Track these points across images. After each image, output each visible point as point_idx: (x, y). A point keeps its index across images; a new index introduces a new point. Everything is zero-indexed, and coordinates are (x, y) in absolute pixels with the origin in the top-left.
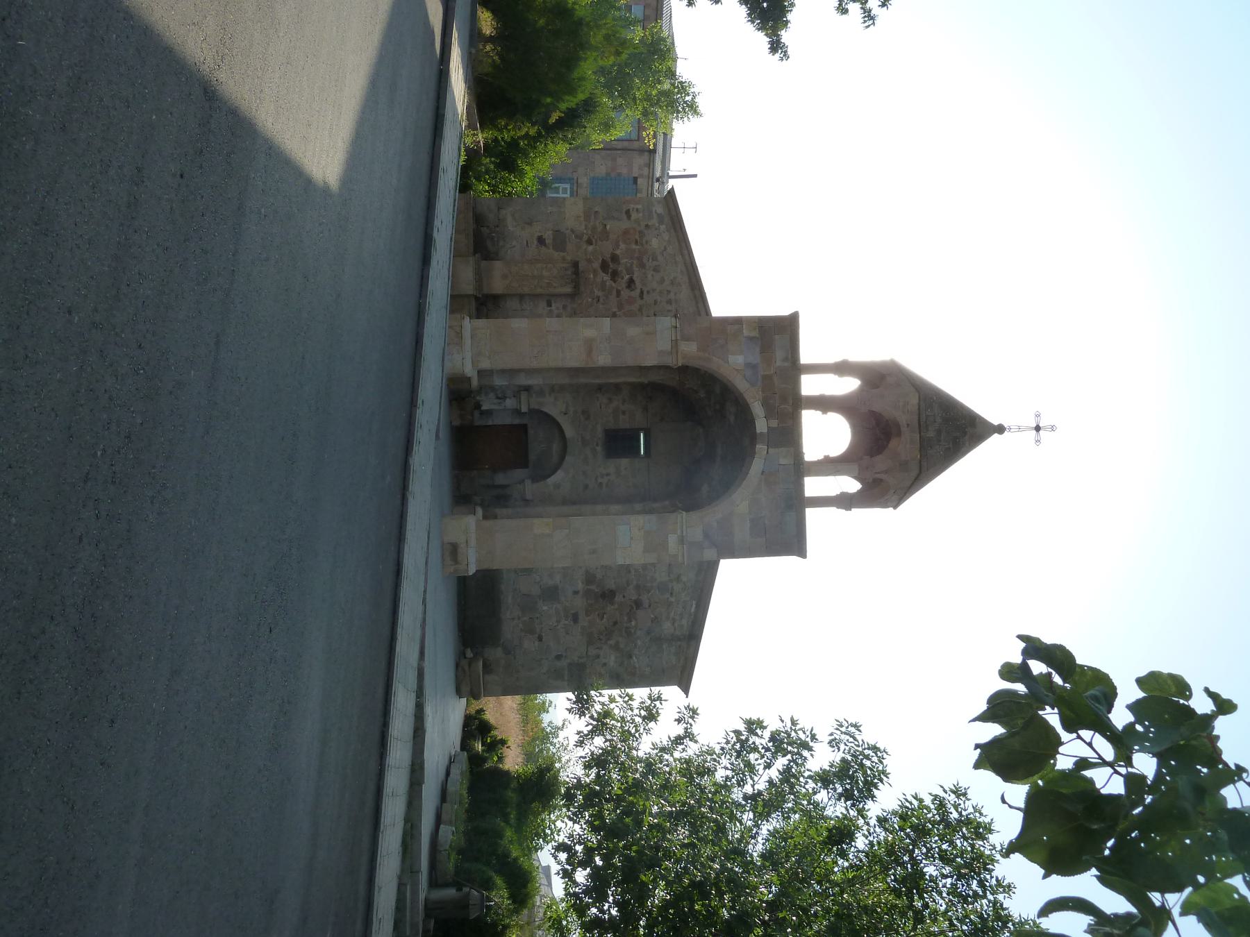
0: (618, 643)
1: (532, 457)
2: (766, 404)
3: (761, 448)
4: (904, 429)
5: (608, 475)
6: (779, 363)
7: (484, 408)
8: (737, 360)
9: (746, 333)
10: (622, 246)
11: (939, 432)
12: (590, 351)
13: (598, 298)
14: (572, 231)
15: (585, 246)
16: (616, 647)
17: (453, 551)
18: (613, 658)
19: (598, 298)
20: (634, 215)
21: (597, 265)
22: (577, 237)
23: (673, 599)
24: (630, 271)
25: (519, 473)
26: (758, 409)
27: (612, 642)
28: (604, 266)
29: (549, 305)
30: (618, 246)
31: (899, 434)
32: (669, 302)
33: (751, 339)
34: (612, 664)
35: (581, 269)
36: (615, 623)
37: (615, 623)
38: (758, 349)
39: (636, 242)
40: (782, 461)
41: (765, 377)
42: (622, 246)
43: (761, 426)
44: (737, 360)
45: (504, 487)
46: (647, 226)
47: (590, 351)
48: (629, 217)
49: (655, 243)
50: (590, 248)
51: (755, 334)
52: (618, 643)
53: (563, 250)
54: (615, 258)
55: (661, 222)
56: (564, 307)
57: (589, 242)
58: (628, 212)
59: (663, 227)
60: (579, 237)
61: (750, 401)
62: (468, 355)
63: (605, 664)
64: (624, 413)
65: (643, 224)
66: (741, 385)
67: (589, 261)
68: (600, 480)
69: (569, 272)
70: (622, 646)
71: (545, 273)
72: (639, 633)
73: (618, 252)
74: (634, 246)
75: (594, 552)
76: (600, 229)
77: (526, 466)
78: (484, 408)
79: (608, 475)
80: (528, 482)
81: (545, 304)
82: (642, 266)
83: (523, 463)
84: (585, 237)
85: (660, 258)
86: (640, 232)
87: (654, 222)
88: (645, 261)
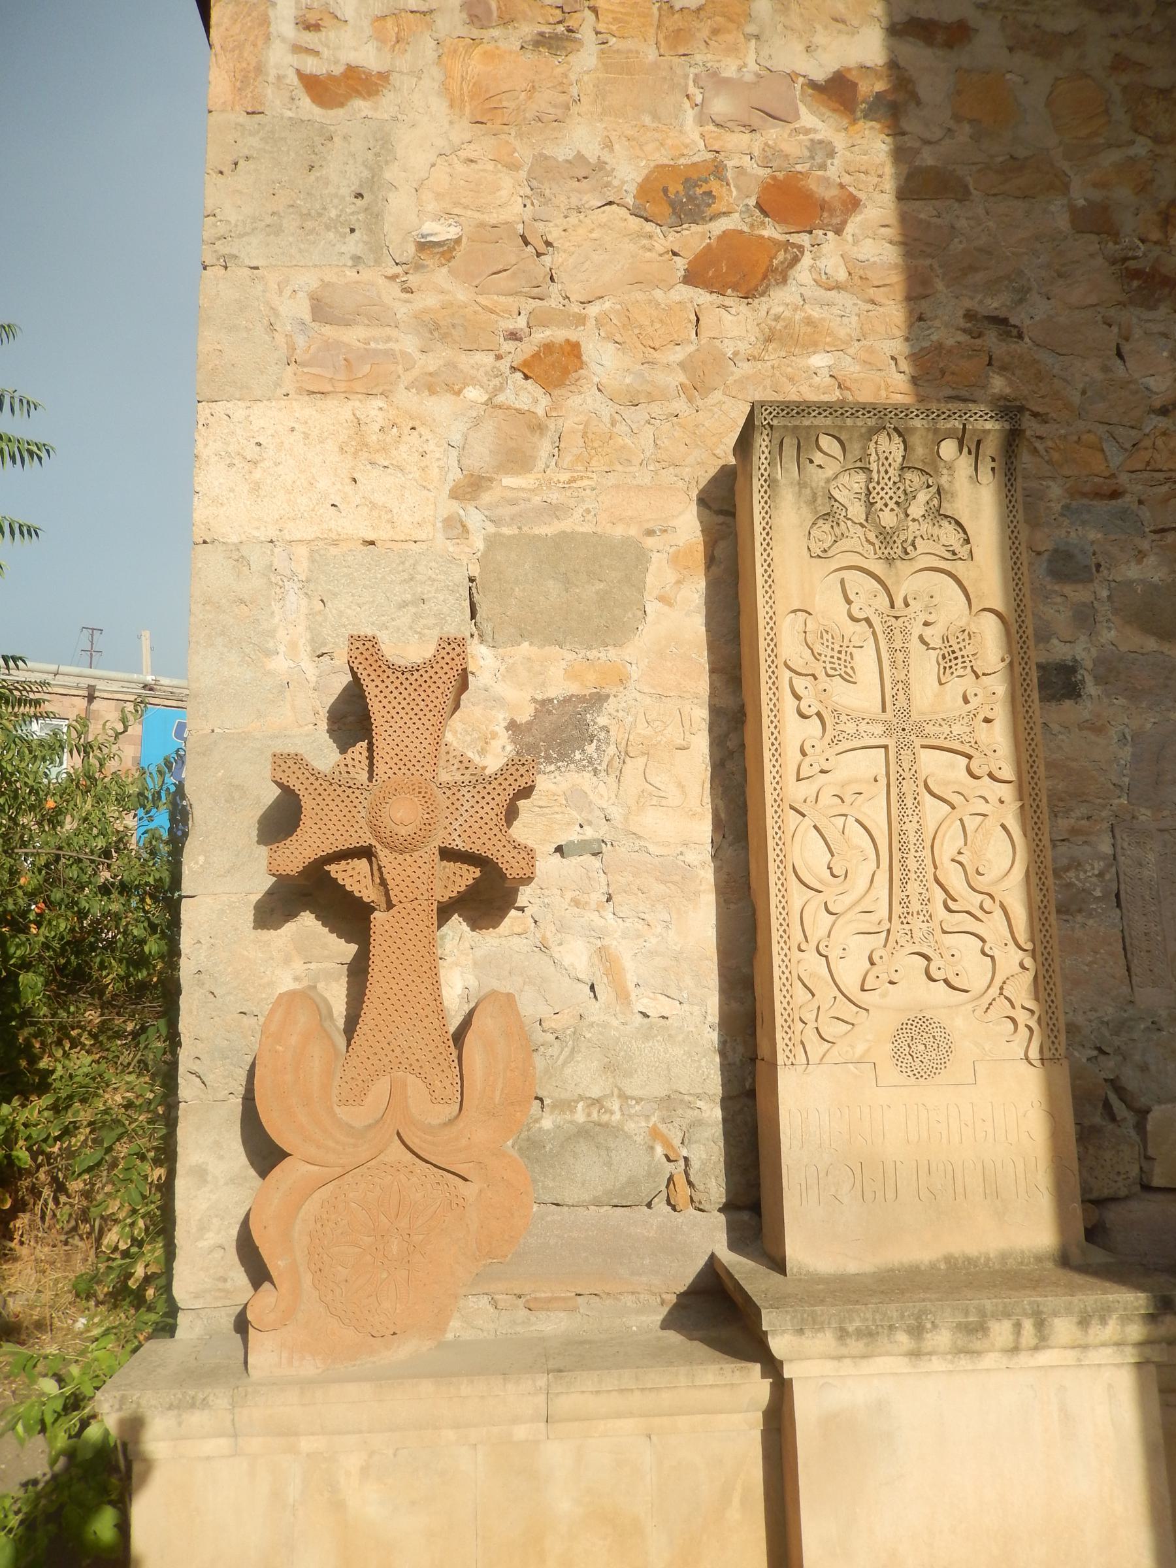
10: (582, 138)
14: (471, 487)
15: (582, 404)
19: (977, 323)
21: (734, 323)
22: (516, 459)
28: (738, 272)
30: (588, 172)
42: (582, 138)
48: (357, 83)
50: (603, 359)
53: (632, 559)
54: (678, 197)
57: (556, 366)
58: (320, 89)
71: (861, 695)
73: (628, 174)
76: (442, 287)
84: (526, 396)
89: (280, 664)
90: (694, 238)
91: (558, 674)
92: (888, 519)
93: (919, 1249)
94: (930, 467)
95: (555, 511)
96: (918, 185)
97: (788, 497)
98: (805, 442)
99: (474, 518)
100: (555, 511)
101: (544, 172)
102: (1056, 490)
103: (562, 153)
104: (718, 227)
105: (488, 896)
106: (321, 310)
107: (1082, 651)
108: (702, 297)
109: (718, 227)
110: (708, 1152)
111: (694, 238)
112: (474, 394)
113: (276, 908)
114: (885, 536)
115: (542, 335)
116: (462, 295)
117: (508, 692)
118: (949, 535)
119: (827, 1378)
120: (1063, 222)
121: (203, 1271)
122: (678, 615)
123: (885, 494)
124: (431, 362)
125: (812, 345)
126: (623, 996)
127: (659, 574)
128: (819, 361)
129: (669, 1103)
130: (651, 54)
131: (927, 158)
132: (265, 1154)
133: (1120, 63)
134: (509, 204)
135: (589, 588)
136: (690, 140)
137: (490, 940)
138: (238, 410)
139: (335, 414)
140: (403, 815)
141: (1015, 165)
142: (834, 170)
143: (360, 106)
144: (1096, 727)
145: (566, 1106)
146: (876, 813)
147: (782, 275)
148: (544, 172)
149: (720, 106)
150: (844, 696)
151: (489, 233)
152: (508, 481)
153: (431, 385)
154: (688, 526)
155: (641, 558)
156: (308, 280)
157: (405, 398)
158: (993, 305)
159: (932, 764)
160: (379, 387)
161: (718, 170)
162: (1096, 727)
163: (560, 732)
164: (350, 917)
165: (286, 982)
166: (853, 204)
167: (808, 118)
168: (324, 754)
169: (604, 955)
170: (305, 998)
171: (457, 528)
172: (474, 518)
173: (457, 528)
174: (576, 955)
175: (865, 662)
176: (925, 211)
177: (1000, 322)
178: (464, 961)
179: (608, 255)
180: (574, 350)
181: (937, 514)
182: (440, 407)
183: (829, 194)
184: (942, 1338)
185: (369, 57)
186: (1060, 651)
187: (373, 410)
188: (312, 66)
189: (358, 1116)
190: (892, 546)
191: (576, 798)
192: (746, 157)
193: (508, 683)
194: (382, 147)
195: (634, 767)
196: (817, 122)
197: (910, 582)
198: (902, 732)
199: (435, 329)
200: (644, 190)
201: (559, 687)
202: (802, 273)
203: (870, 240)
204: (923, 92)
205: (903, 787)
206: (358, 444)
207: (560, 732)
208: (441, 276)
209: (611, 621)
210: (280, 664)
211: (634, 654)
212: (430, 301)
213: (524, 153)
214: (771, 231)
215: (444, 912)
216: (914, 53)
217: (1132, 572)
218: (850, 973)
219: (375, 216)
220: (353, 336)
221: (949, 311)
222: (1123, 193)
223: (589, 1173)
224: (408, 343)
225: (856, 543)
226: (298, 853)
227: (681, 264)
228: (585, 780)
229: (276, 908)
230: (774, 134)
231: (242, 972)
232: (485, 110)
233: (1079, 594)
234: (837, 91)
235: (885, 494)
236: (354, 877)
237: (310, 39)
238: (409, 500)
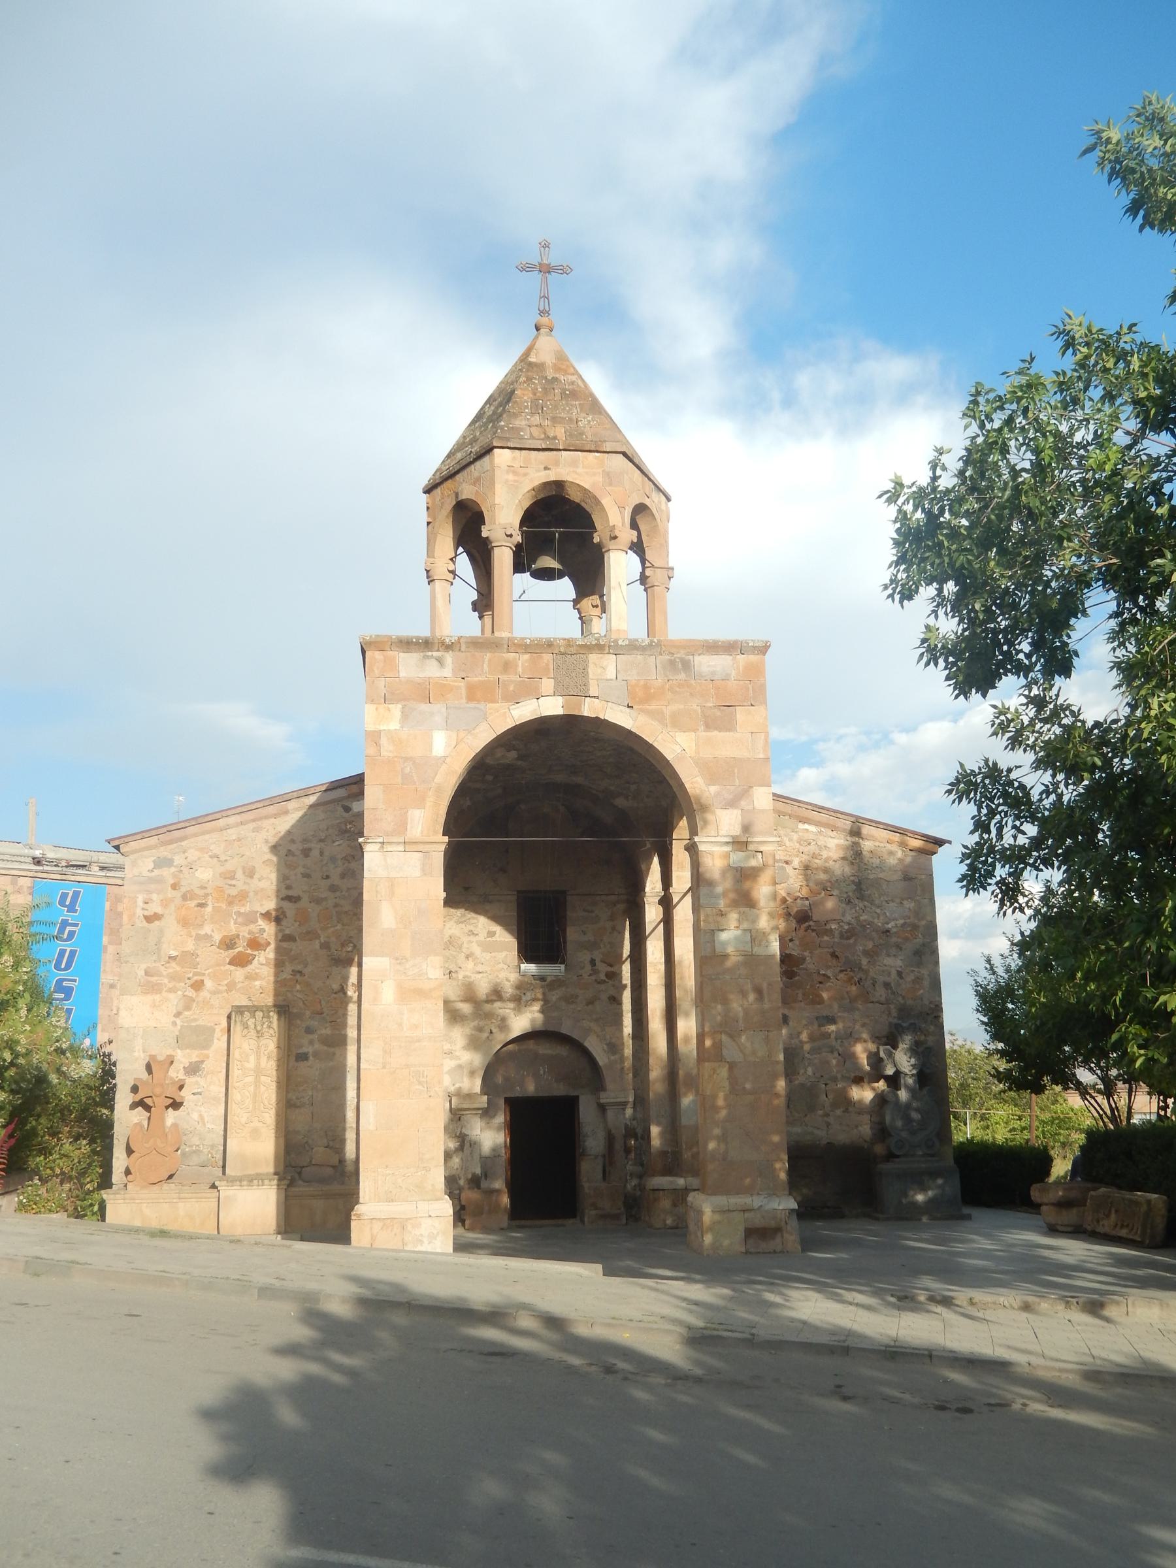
0: (866, 953)
1: (560, 1090)
2: (515, 698)
3: (588, 709)
4: (552, 476)
5: (593, 962)
6: (447, 672)
7: (478, 1171)
8: (440, 743)
9: (394, 725)
10: (207, 929)
11: (555, 420)
12: (421, 993)
13: (295, 972)
14: (178, 1015)
15: (204, 994)
16: (871, 954)
17: (760, 1234)
18: (889, 961)
19: (295, 972)
20: (155, 908)
21: (239, 973)
22: (188, 1008)
23: (796, 862)
24: (250, 919)
25: (587, 1112)
26: (525, 712)
27: (864, 961)
28: (240, 961)
29: (302, 1057)
30: (207, 937)
31: (559, 485)
32: (306, 853)
33: (405, 716)
34: (899, 963)
35: (243, 1001)
36: (834, 955)
37: (834, 955)
38: (424, 707)
39: (201, 905)
40: (611, 673)
41: (471, 697)
43: (552, 706)
44: (440, 743)
45: (610, 1139)
46: (174, 887)
47: (421, 993)
49: (205, 874)
50: (209, 984)
51: (396, 709)
52: (866, 953)
53: (212, 1030)
54: (228, 943)
55: (168, 862)
56: (309, 1031)
57: (198, 986)
58: (149, 919)
59: (178, 860)
60: (188, 1004)
61: (510, 724)
62: (424, 1207)
63: (900, 974)
64: (491, 934)
65: (170, 893)
66: (482, 737)
67: (231, 987)
68: (602, 977)
69: (251, 1022)
70: (870, 945)
71: (251, 1063)
72: (848, 918)
73: (217, 937)
74: (209, 909)
75: (759, 991)
76: (175, 967)
77: (577, 1097)
78: (478, 1171)
79: (593, 962)
80: (604, 1098)
81: (302, 1064)
82: (243, 896)
83: (569, 1105)
84: (191, 993)
85: (229, 866)
86: (185, 898)
87: (167, 873)
88: (233, 892)
89: (136, 1054)
90: (232, 953)
91: (194, 1056)
92: (259, 1028)
93: (251, 1172)
94: (269, 1017)
95: (195, 1020)
96: (284, 939)
97: (238, 1024)
98: (242, 1013)
99: (178, 1021)
100: (195, 1020)
101: (199, 938)
102: (308, 1013)
103: (203, 933)
104: (237, 950)
105: (176, 1105)
106: (147, 973)
107: (310, 1050)
108: (232, 968)
109: (237, 950)
110: (219, 1156)
111: (232, 953)
112: (179, 993)
113: (134, 1106)
114: (258, 1032)
115: (195, 978)
116: (178, 969)
117: (183, 1060)
118: (271, 1031)
119: (226, 1191)
120: (318, 947)
121: (117, 1176)
122: (220, 1043)
123: (258, 1023)
124: (170, 985)
125: (256, 979)
126: (204, 1124)
127: (218, 1033)
128: (257, 983)
129: (213, 1146)
130: (224, 906)
131: (287, 932)
132: (130, 1151)
133: (336, 905)
134: (190, 946)
135: (202, 1037)
136: (233, 929)
137: (177, 1112)
138: (129, 997)
139: (150, 998)
140: (158, 1090)
141: (308, 933)
142: (265, 935)
143: (157, 923)
144: (310, 1067)
145: (191, 1146)
146: (252, 1088)
147: (250, 962)
148: (199, 938)
149: (240, 920)
150: (247, 1065)
151: (185, 953)
152: (187, 1013)
153: (170, 990)
154: (224, 1024)
155: (214, 1030)
156: (144, 966)
157: (164, 994)
158: (299, 968)
159: (263, 1078)
160: (159, 991)
161: (238, 936)
162: (310, 1067)
163: (193, 1069)
164: (148, 1108)
165: (136, 1121)
166: (269, 944)
167: (260, 922)
168: (144, 1075)
169: (201, 1116)
170: (139, 1124)
171: (174, 1024)
172: (178, 1021)
173: (174, 1024)
174: (195, 1116)
175: (252, 1058)
176: (285, 945)
177: (300, 972)
178: (171, 1116)
179: (211, 957)
180: (202, 981)
181: (269, 1027)
182: (172, 996)
183: (263, 942)
184: (245, 1183)
185: (159, 910)
186: (305, 1050)
187: (157, 997)
188: (146, 913)
189: (147, 1145)
190: (259, 1034)
191: (197, 1083)
192: (244, 932)
193: (183, 1058)
194: (161, 931)
195: (209, 1076)
196: (262, 923)
197: (263, 1042)
198: (258, 1072)
199: (172, 978)
200: (220, 942)
201: (194, 1059)
202: (255, 962)
203: (270, 953)
204: (288, 914)
205: (257, 1083)
206: (154, 1006)
207: (193, 1069)
208: (173, 964)
209: (206, 1044)
210: (136, 1054)
211: (211, 1052)
212: (171, 970)
213: (194, 934)
214: (249, 951)
215: (167, 1108)
216: (286, 904)
217: (324, 1031)
218: (244, 1120)
219: (159, 950)
220: (154, 979)
221: (289, 968)
222: (333, 939)
223: (195, 1160)
224: (166, 981)
225: (253, 1033)
226: (138, 1097)
227: (228, 960)
228: (199, 1079)
229: (134, 1106)
230: (252, 927)
231: (125, 1118)
232: (185, 923)
233: (311, 1037)
234: (266, 915)
235: (258, 1023)
236: (148, 1101)
237: (146, 906)
238: (164, 1018)
